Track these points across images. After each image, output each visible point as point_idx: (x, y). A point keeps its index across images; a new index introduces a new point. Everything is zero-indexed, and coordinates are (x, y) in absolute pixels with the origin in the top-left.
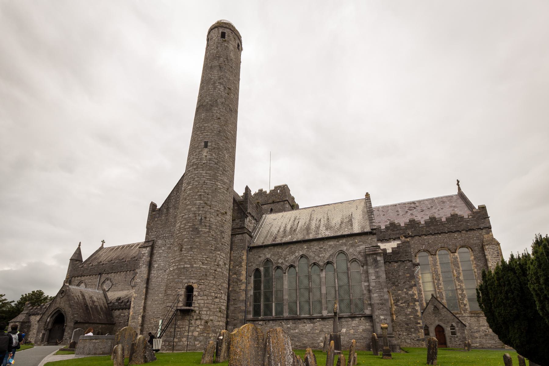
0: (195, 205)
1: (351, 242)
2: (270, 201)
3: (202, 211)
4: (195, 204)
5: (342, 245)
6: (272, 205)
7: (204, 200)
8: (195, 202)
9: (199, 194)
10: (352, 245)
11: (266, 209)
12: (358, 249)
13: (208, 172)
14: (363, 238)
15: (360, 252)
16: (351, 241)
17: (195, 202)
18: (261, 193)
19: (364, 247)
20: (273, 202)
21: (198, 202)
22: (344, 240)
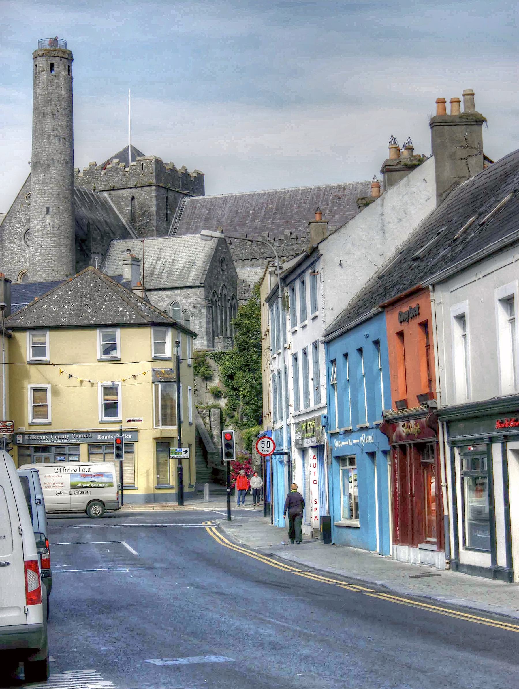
0: (45, 272)
1: (184, 293)
2: (131, 184)
3: (51, 277)
4: (45, 271)
5: (176, 295)
6: (134, 190)
7: (51, 267)
8: (44, 269)
9: (47, 261)
10: (185, 297)
11: (124, 197)
12: (189, 301)
13: (52, 239)
14: (194, 290)
15: (191, 304)
16: (184, 292)
17: (44, 269)
18: (117, 169)
19: (194, 298)
20: (136, 187)
21: (47, 269)
22: (179, 291)
